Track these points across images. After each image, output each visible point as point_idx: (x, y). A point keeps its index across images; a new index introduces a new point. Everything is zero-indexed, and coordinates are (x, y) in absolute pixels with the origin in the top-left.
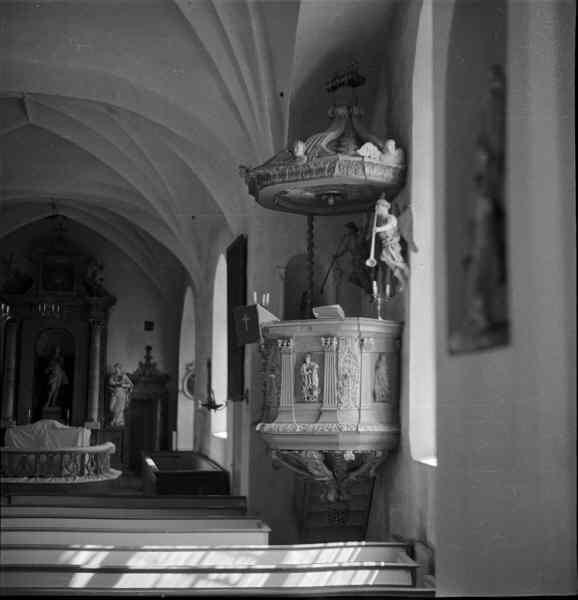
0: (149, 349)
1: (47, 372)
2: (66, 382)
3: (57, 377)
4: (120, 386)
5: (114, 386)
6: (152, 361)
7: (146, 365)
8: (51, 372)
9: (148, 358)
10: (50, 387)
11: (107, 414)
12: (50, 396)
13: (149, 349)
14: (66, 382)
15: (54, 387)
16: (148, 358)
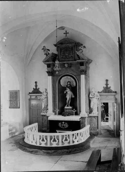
0: (107, 81)
1: (65, 92)
2: (73, 97)
3: (69, 94)
4: (94, 97)
5: (92, 98)
6: (109, 86)
7: (106, 88)
8: (67, 92)
9: (107, 84)
10: (66, 99)
11: (91, 111)
12: (67, 102)
13: (107, 81)
14: (73, 97)
15: (68, 99)
16: (107, 84)
